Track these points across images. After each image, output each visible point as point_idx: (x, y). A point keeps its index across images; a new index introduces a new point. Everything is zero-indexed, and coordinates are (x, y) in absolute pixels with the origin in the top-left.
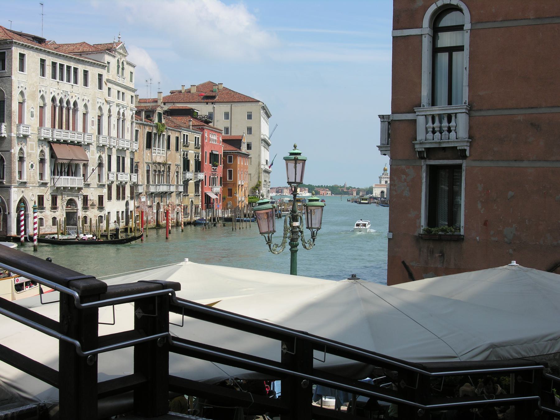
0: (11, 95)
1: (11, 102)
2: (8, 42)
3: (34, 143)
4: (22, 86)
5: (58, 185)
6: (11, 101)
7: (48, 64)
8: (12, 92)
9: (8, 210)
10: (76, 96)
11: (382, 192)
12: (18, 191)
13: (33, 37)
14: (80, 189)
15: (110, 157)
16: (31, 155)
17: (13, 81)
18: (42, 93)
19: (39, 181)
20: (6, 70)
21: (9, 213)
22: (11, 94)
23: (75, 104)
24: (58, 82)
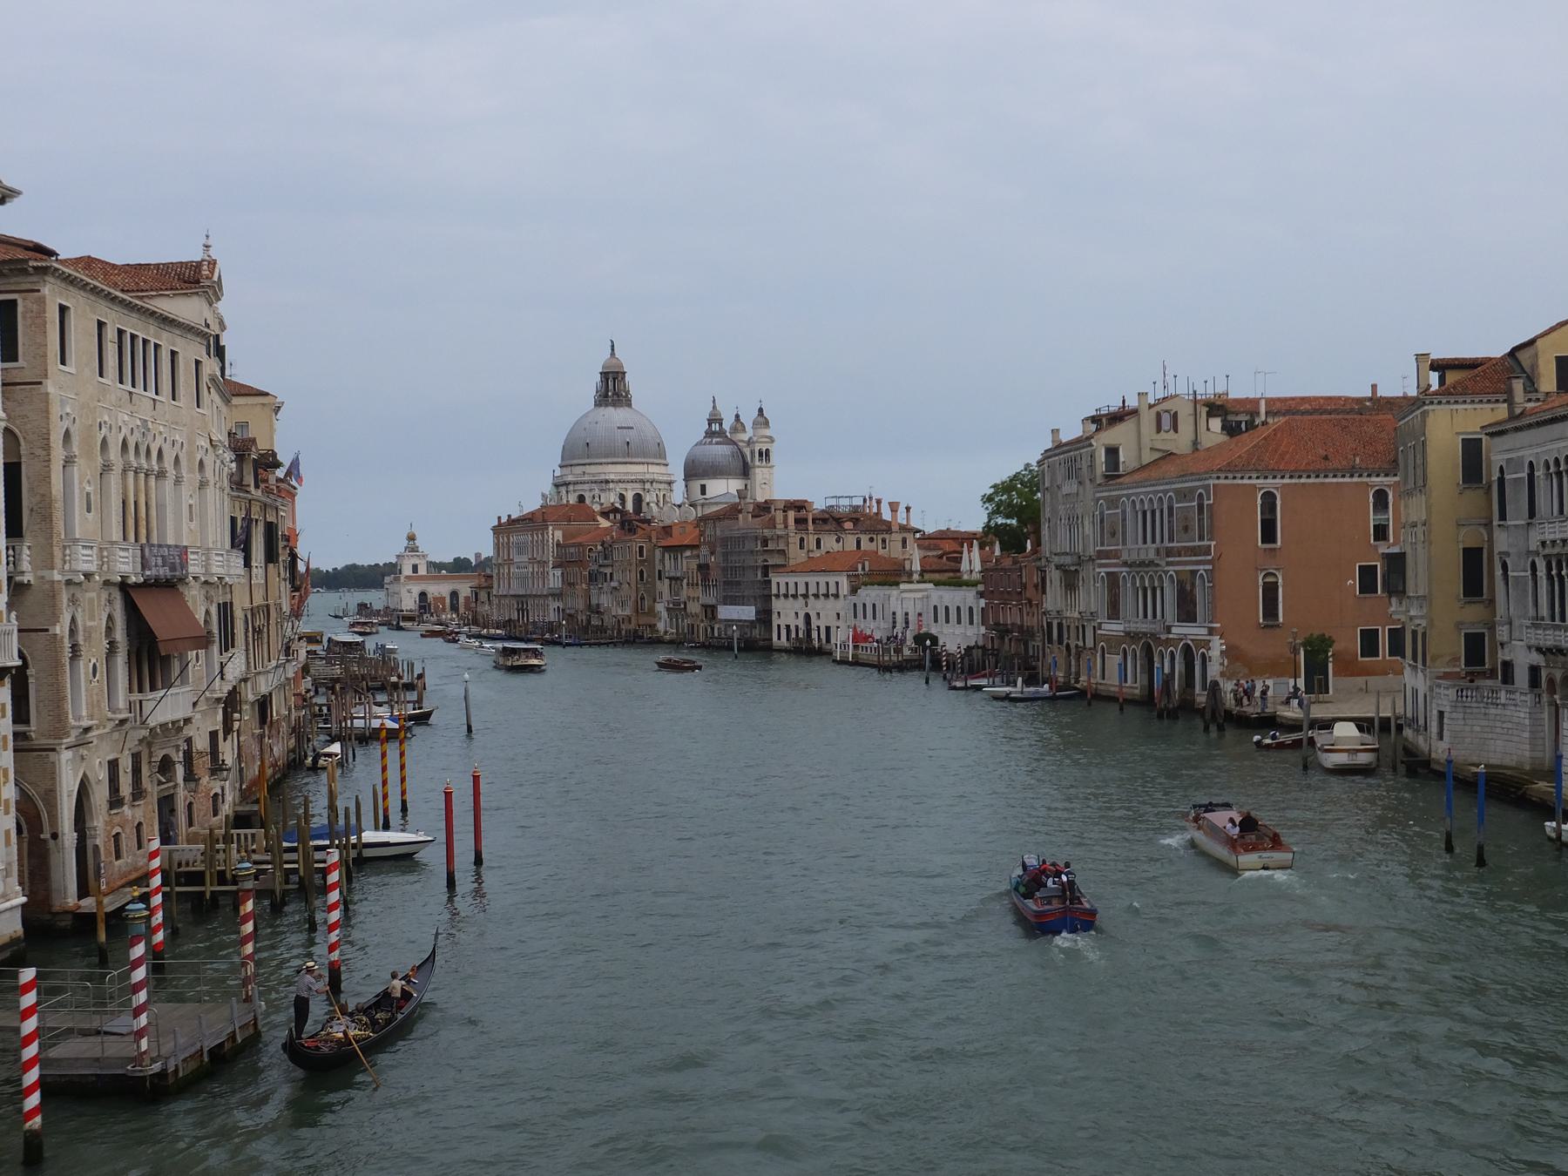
0: (48, 445)
1: (49, 466)
2: (30, 269)
3: (94, 595)
4: (67, 414)
5: (152, 722)
6: (46, 464)
7: (111, 334)
8: (49, 434)
9: (51, 826)
10: (161, 433)
11: (423, 595)
12: (74, 757)
13: (31, 245)
14: (187, 721)
15: (219, 604)
16: (90, 634)
17: (51, 396)
18: (104, 429)
19: (110, 715)
20: (21, 362)
21: (55, 836)
22: (45, 442)
23: (160, 452)
24: (130, 393)
